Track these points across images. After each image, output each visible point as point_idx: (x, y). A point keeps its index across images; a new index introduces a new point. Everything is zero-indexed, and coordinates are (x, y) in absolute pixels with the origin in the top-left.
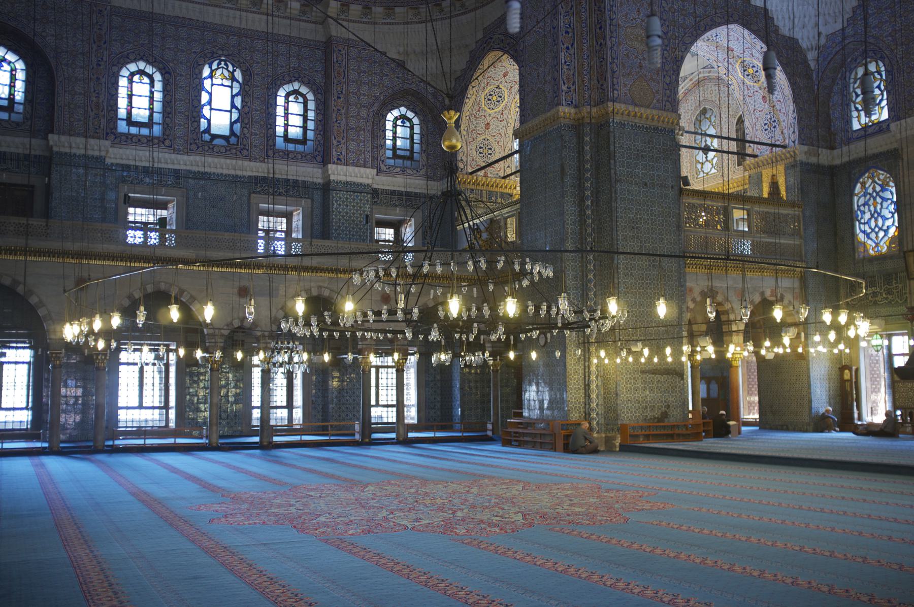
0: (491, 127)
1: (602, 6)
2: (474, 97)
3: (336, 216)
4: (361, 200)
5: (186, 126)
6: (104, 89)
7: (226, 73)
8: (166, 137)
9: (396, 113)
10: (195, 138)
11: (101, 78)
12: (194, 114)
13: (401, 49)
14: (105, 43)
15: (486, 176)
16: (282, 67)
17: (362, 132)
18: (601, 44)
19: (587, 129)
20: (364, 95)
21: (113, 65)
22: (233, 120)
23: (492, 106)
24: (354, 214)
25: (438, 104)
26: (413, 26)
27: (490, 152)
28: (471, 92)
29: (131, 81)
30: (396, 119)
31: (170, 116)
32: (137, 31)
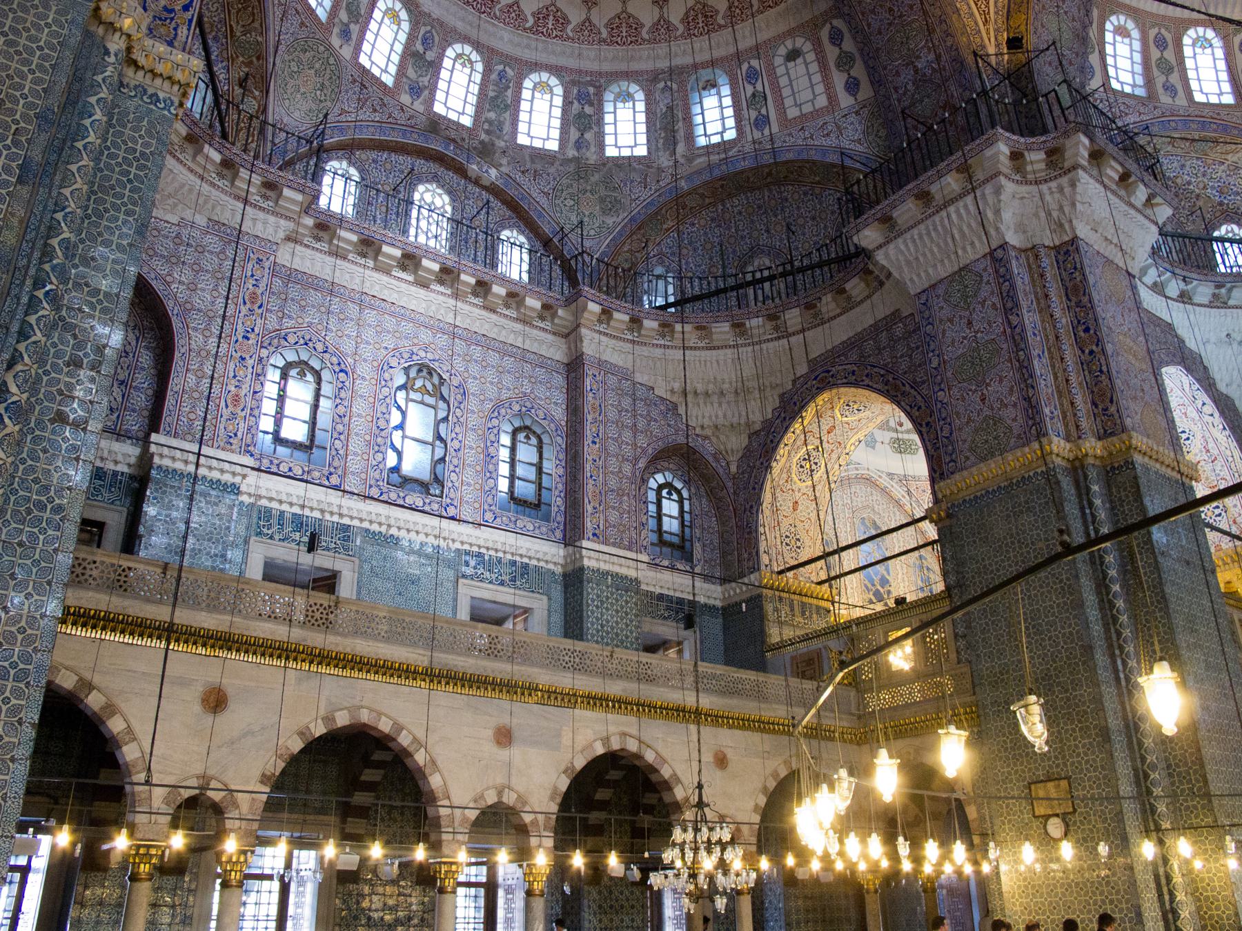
0: (800, 508)
1: (1085, 299)
2: (783, 460)
3: (593, 624)
4: (627, 602)
5: (366, 457)
6: (249, 376)
7: (430, 387)
8: (332, 470)
9: (660, 478)
10: (377, 477)
11: (247, 357)
12: (379, 440)
13: (677, 386)
14: (260, 307)
15: (796, 577)
16: (509, 389)
17: (625, 498)
18: (1091, 352)
19: (1092, 474)
20: (627, 444)
21: (262, 347)
22: (436, 458)
23: (803, 477)
24: (617, 623)
25: (721, 471)
26: (697, 353)
27: (799, 544)
28: (781, 452)
29: (284, 376)
30: (661, 487)
31: (342, 437)
32: (303, 303)
